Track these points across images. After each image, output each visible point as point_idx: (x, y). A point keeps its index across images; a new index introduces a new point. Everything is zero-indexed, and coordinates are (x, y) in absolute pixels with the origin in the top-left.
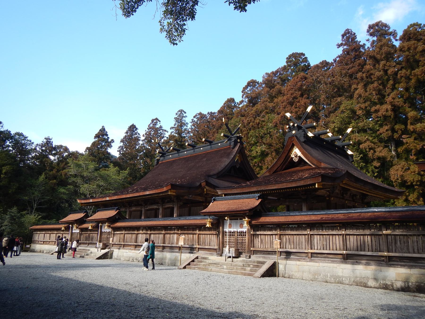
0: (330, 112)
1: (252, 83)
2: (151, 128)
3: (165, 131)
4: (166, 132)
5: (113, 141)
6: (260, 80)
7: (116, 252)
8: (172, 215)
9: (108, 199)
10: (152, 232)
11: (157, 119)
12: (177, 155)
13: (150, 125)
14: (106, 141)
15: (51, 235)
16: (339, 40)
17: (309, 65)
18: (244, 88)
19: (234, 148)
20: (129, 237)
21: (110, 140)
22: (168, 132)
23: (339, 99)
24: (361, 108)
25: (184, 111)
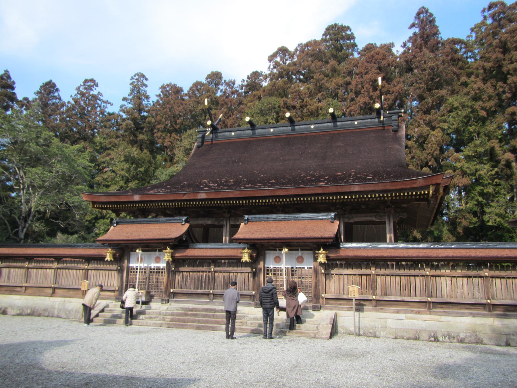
0: (432, 108)
1: (283, 51)
2: (83, 94)
3: (107, 102)
4: (109, 105)
5: (26, 99)
6: (291, 49)
7: (347, 318)
8: (219, 240)
9: (202, 196)
10: (497, 273)
11: (92, 80)
12: (250, 132)
13: (79, 88)
14: (13, 98)
15: (34, 271)
16: (412, 20)
17: (354, 45)
18: (272, 56)
19: (396, 131)
20: (388, 281)
21: (20, 98)
22: (112, 105)
23: (443, 92)
24: (483, 108)
25: (143, 76)
